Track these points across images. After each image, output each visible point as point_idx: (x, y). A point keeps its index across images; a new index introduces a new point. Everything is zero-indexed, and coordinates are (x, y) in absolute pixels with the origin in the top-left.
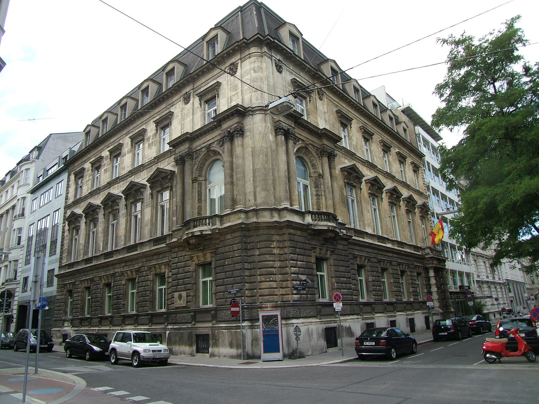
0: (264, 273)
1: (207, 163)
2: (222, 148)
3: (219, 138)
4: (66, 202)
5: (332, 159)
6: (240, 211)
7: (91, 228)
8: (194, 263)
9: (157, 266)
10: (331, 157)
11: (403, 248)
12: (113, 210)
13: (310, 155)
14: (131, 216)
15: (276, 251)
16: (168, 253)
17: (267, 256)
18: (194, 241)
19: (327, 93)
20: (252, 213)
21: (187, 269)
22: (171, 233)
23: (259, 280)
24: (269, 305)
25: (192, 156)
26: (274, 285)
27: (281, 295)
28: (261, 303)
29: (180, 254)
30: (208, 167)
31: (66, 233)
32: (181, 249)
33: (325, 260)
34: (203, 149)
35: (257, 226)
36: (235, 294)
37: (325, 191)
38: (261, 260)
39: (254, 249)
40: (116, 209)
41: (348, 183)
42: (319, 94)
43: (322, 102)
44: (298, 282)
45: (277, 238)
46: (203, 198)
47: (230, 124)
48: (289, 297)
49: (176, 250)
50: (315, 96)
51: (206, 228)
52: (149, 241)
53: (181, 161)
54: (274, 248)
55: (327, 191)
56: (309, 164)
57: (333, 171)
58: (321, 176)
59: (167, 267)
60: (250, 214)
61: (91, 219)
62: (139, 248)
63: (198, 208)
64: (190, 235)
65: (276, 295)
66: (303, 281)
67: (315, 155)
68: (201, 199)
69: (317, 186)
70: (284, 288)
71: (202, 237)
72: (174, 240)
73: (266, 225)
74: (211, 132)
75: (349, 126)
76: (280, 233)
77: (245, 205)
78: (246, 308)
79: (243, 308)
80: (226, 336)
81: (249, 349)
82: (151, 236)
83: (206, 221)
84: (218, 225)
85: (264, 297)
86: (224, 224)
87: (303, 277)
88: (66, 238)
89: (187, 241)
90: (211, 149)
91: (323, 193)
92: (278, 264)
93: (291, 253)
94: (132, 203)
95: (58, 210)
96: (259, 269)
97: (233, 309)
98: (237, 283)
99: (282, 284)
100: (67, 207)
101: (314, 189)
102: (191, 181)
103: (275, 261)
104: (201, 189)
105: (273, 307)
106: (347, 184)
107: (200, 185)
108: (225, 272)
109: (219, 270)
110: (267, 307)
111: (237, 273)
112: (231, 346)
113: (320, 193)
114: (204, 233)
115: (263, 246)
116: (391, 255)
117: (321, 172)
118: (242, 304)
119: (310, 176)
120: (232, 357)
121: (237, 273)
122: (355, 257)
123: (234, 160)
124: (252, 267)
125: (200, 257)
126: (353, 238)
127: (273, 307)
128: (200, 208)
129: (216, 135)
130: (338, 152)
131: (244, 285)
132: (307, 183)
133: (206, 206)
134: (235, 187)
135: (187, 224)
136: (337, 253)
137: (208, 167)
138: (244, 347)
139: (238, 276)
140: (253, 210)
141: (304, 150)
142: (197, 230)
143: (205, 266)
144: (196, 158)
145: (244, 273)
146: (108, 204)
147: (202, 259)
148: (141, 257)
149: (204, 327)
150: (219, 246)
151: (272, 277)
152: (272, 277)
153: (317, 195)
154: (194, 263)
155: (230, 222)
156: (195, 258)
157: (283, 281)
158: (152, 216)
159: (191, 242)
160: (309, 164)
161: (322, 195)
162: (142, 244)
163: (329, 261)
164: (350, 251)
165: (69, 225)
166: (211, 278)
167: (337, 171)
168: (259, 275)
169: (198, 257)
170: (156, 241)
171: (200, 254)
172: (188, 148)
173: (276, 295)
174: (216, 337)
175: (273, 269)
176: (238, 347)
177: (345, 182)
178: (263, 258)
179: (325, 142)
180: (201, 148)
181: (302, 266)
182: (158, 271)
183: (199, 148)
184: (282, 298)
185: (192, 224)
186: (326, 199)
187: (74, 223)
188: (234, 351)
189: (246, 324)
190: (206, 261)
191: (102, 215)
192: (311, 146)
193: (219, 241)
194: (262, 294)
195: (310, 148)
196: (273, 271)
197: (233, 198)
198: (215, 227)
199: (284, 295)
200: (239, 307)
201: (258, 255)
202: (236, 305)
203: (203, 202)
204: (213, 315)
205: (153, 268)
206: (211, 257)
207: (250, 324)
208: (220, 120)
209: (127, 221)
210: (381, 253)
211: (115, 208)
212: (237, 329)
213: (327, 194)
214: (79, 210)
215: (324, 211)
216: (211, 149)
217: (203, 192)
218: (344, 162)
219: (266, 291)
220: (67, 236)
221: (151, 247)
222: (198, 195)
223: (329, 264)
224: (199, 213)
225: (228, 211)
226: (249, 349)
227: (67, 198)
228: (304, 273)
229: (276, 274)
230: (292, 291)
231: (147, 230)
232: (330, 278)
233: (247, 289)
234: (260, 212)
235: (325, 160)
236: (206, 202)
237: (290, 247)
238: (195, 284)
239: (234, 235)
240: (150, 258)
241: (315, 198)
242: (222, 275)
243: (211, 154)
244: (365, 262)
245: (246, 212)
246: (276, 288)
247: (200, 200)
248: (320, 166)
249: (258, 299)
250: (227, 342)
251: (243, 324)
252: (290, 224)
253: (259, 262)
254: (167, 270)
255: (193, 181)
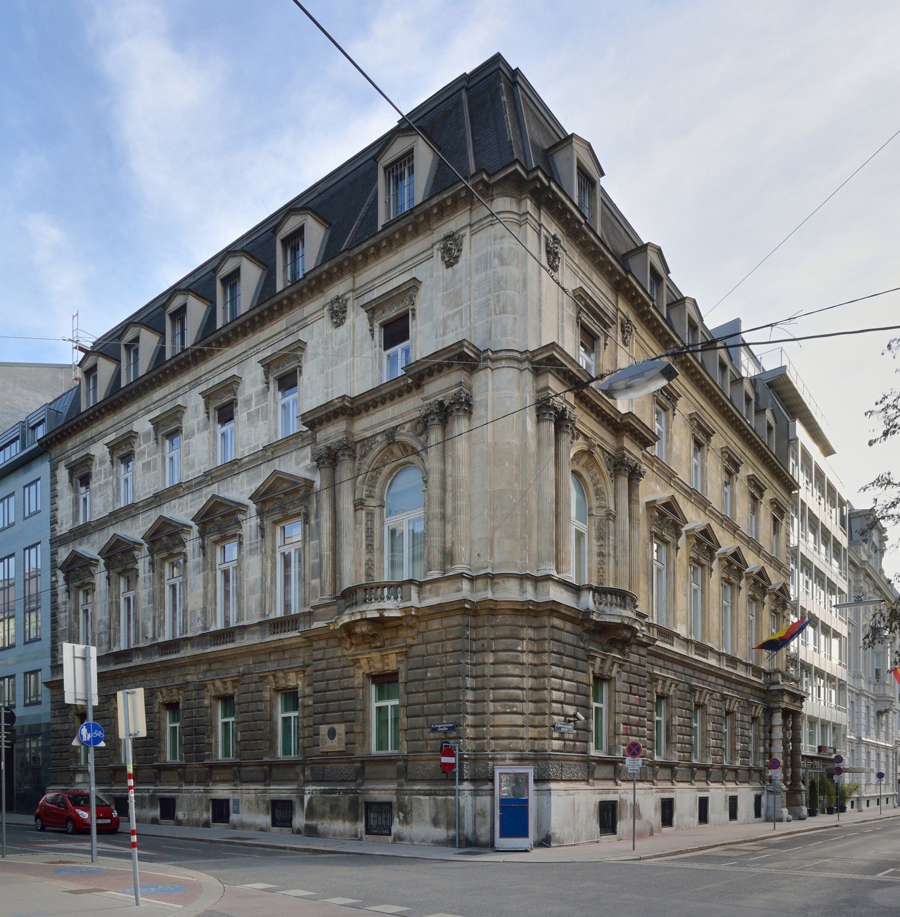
0: (502, 697)
1: (386, 470)
2: (422, 438)
3: (416, 414)
4: (53, 530)
5: (634, 481)
6: (461, 576)
7: (122, 590)
8: (361, 672)
9: (280, 674)
10: (634, 475)
11: (736, 669)
12: (172, 555)
13: (595, 470)
14: (213, 569)
15: (526, 658)
16: (301, 651)
17: (509, 666)
18: (364, 629)
19: (639, 330)
20: (484, 581)
21: (345, 683)
22: (307, 609)
23: (492, 710)
24: (508, 756)
25: (354, 451)
26: (518, 719)
27: (531, 738)
28: (493, 751)
29: (330, 653)
30: (387, 479)
31: (62, 598)
32: (333, 642)
33: (605, 680)
34: (379, 438)
35: (492, 609)
36: (445, 732)
37: (615, 548)
38: (497, 673)
39: (485, 651)
40: (180, 554)
41: (656, 535)
42: (623, 332)
43: (627, 349)
44: (563, 718)
45: (531, 633)
46: (376, 544)
47: (440, 387)
48: (544, 744)
49: (322, 644)
50: (615, 333)
51: (392, 608)
52: (259, 624)
53: (329, 459)
54: (522, 652)
55: (620, 548)
56: (591, 489)
57: (634, 506)
58: (611, 516)
59: (302, 675)
60: (480, 584)
61: (119, 570)
62: (237, 637)
63: (367, 564)
64: (359, 617)
65: (522, 739)
66: (570, 716)
67: (604, 469)
68: (372, 545)
69: (601, 537)
70: (535, 727)
71: (381, 622)
72: (316, 625)
73: (511, 607)
74: (397, 399)
75: (671, 410)
76: (535, 625)
77: (470, 565)
78: (467, 759)
79: (461, 759)
80: (425, 805)
81: (468, 829)
82: (264, 615)
83: (382, 591)
84: (414, 601)
85: (500, 742)
86: (424, 599)
87: (570, 710)
88: (62, 608)
89: (349, 628)
90: (397, 438)
91: (612, 552)
92: (528, 682)
93: (553, 664)
94: (216, 542)
95: (35, 545)
96: (493, 689)
97: (445, 760)
98: (448, 714)
99: (533, 720)
100: (57, 542)
101: (594, 542)
102: (352, 507)
103: (522, 677)
104: (372, 524)
105: (514, 759)
106: (656, 536)
107: (370, 514)
108: (427, 692)
109: (412, 687)
110: (503, 759)
111: (450, 695)
112: (435, 822)
113: (605, 552)
114: (386, 614)
115: (502, 647)
116: (713, 679)
117: (612, 507)
118: (460, 750)
119: (591, 515)
120: (437, 843)
121: (450, 695)
122: (654, 679)
123: (449, 468)
124: (480, 685)
125: (373, 660)
126: (658, 643)
127: (514, 759)
128: (370, 565)
129: (408, 408)
130: (648, 471)
131: (465, 718)
132: (583, 528)
133: (382, 561)
134: (449, 527)
135: (348, 597)
136: (628, 669)
137: (387, 479)
138: (461, 826)
139: (453, 701)
140: (486, 576)
141: (585, 458)
142: (371, 611)
143: (384, 681)
144: (363, 456)
145: (464, 695)
146: (160, 539)
147: (379, 666)
148: (242, 655)
149: (381, 792)
150: (415, 642)
151: (515, 706)
152: (515, 706)
153: (601, 554)
154: (361, 672)
155: (438, 595)
156: (364, 662)
157: (536, 714)
158: (264, 574)
159: (358, 630)
160: (591, 489)
161: (609, 555)
162: (244, 628)
163: (613, 683)
164: (649, 668)
165: (66, 579)
166: (396, 702)
167: (641, 510)
168: (493, 701)
169: (369, 660)
170: (277, 625)
171: (376, 655)
172: (346, 432)
173: (522, 739)
174: (406, 807)
175: (519, 692)
176: (449, 825)
177: (651, 532)
178: (501, 669)
179: (627, 443)
180: (374, 436)
181: (571, 690)
182: (282, 683)
183: (368, 434)
184: (533, 745)
185: (360, 595)
186: (616, 563)
187: (78, 577)
188: (441, 833)
189: (466, 786)
190: (386, 668)
191: (147, 565)
192: (598, 449)
193: (414, 632)
194: (497, 735)
195: (598, 454)
196: (518, 695)
197: (444, 548)
198: (408, 604)
199: (536, 739)
200: (453, 755)
201: (492, 664)
202: (449, 753)
203: (376, 553)
204: (402, 769)
205: (271, 677)
206: (398, 662)
207: (473, 788)
208: (419, 375)
209: (206, 582)
210: (697, 674)
211: (176, 551)
212: (447, 795)
213: (619, 554)
214: (91, 548)
215: (611, 586)
216: (397, 438)
217: (377, 531)
218: (652, 490)
219: (505, 731)
220: (65, 603)
221: (263, 636)
222: (367, 537)
223: (613, 688)
224: (368, 575)
225: (435, 574)
226: (468, 829)
227: (54, 522)
228: (572, 702)
229: (523, 701)
230: (551, 732)
231: (252, 602)
232: (613, 715)
233: (467, 726)
234: (500, 581)
235: (624, 481)
236: (382, 552)
237: (553, 652)
238: (362, 710)
239: (448, 622)
240: (263, 658)
241: (595, 559)
242: (420, 697)
243: (395, 449)
244: (669, 690)
245: (472, 579)
246: (522, 726)
247: (370, 546)
248: (611, 495)
249: (488, 744)
250: (427, 817)
251: (461, 787)
252: (554, 609)
253: (493, 676)
254: (300, 683)
255: (355, 506)
